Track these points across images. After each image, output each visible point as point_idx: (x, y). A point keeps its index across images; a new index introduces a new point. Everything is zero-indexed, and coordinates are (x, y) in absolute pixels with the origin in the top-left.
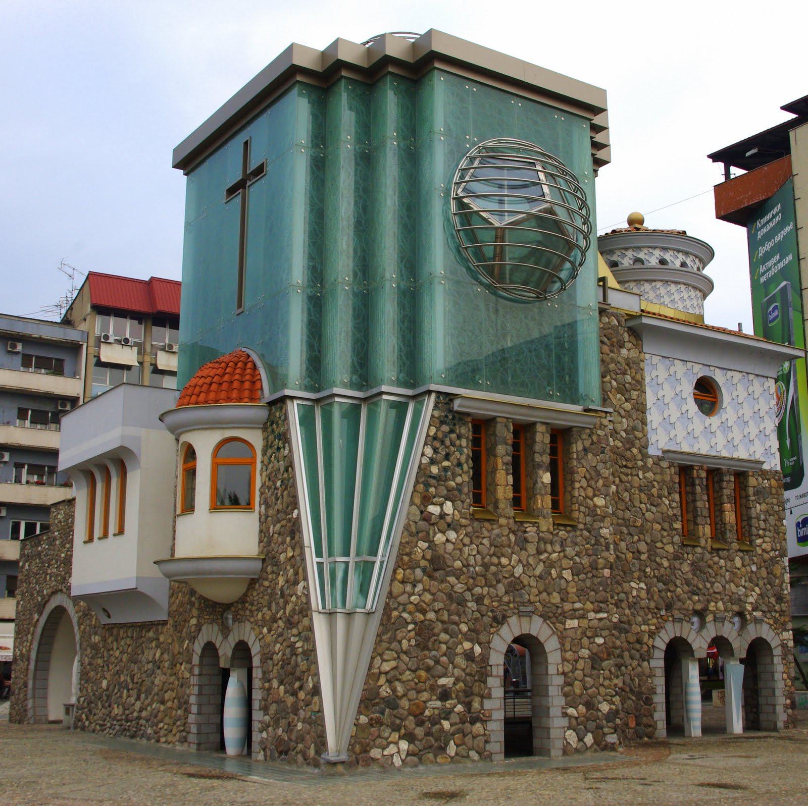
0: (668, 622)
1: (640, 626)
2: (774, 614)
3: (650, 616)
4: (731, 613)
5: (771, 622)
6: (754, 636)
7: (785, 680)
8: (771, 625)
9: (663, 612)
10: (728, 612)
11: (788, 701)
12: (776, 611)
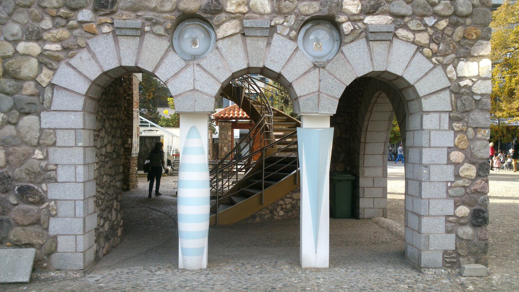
0: (100, 39)
1: (15, 42)
2: (430, 21)
3: (47, 23)
4: (292, 19)
5: (423, 38)
6: (363, 69)
7: (457, 165)
8: (420, 47)
9: (85, 15)
10: (285, 15)
11: (464, 211)
12: (440, 17)
